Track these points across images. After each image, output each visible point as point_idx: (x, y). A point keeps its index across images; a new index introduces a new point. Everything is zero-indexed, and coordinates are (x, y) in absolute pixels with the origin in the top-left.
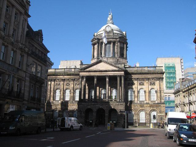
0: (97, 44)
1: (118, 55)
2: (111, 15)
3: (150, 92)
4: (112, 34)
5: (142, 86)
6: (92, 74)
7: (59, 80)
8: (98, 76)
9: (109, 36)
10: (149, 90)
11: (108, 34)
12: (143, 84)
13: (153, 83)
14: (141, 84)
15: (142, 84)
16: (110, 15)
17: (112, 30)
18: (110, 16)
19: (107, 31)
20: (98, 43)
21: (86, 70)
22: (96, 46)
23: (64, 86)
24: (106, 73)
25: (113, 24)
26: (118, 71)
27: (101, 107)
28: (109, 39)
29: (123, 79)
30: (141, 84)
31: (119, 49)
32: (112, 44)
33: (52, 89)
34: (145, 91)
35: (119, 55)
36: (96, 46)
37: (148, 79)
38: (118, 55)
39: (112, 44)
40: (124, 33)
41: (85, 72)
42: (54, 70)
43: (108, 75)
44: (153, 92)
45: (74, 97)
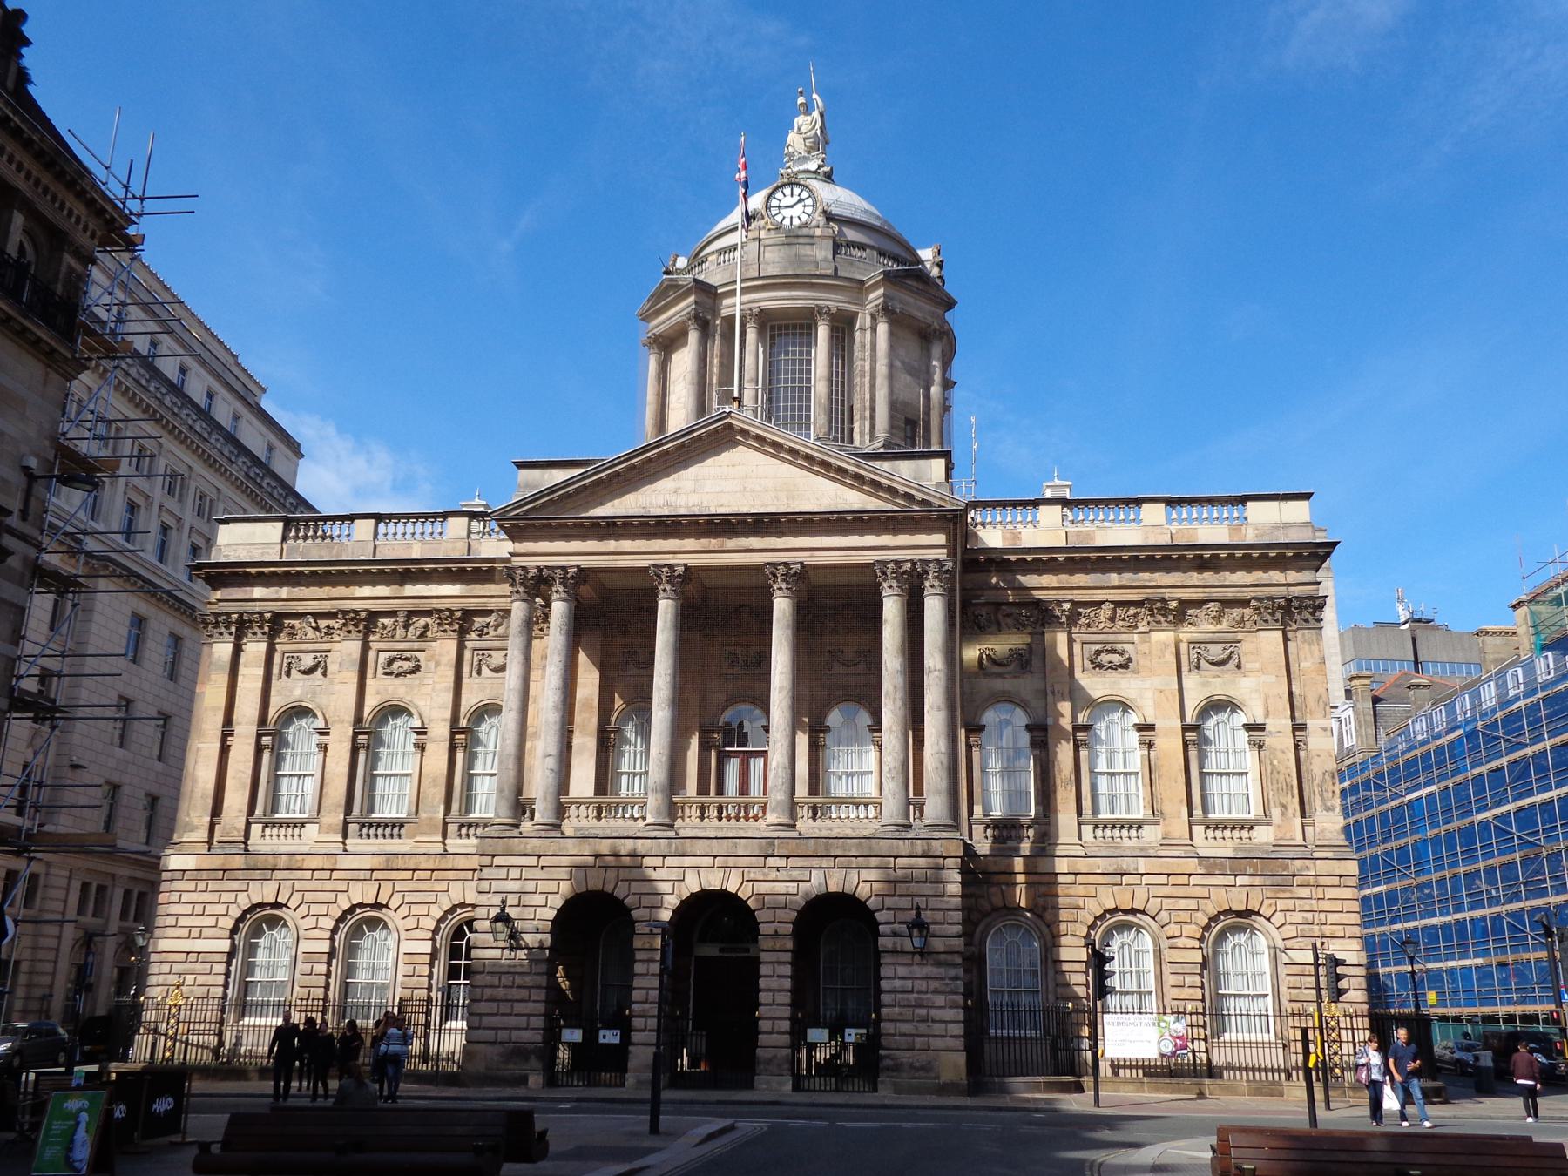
0: (693, 337)
1: (873, 427)
2: (816, 114)
3: (1194, 736)
5: (1112, 677)
7: (323, 623)
9: (798, 260)
10: (1190, 719)
12: (1125, 666)
14: (1104, 658)
15: (1116, 658)
16: (807, 109)
18: (806, 123)
20: (705, 327)
22: (684, 361)
23: (369, 682)
25: (828, 177)
27: (713, 881)
29: (934, 609)
30: (1104, 658)
32: (823, 332)
33: (247, 708)
34: (1150, 727)
36: (684, 361)
38: (873, 427)
39: (823, 332)
40: (926, 254)
44: (1226, 734)
45: (457, 791)
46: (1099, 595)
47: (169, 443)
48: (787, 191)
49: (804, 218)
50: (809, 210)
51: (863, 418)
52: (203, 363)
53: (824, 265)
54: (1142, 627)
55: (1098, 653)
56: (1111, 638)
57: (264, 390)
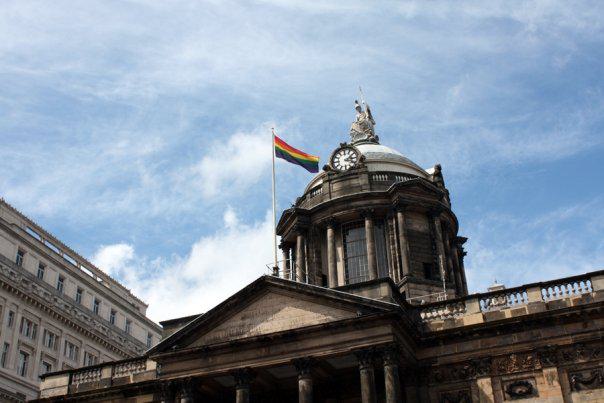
4: (362, 181)
6: (223, 366)
8: (251, 372)
11: (347, 183)
13: (587, 375)
14: (518, 390)
17: (362, 159)
19: (338, 172)
21: (194, 345)
24: (293, 346)
26: (356, 324)
28: (353, 204)
30: (518, 390)
31: (402, 240)
35: (406, 270)
37: (549, 356)
41: (181, 357)
42: (64, 380)
43: (303, 355)
46: (508, 350)
47: (86, 341)
48: (342, 153)
49: (352, 165)
50: (354, 160)
51: (396, 268)
52: (108, 298)
53: (364, 187)
54: (538, 367)
55: (511, 387)
56: (519, 376)
57: (147, 306)
